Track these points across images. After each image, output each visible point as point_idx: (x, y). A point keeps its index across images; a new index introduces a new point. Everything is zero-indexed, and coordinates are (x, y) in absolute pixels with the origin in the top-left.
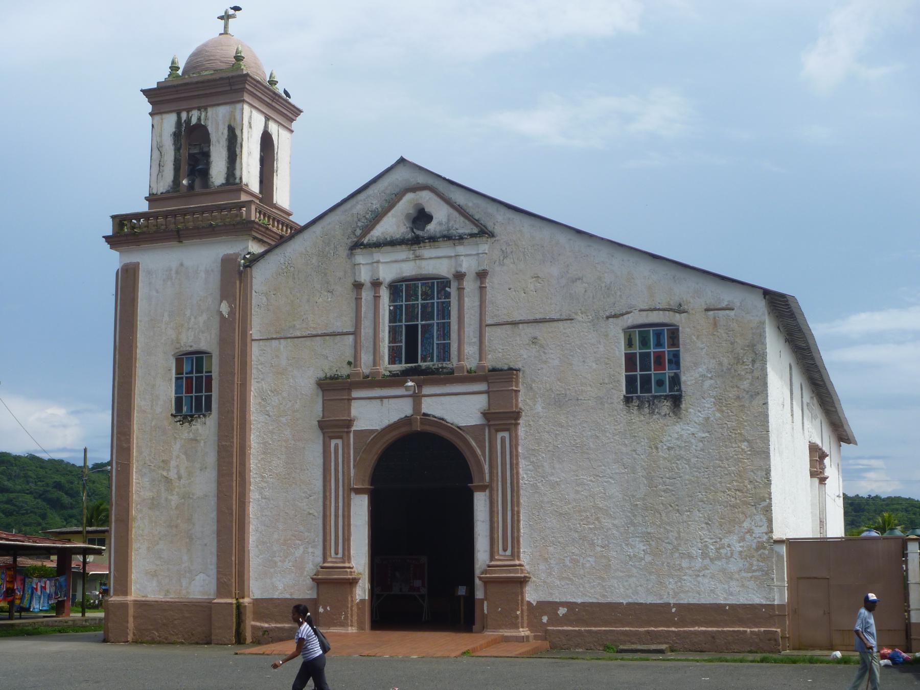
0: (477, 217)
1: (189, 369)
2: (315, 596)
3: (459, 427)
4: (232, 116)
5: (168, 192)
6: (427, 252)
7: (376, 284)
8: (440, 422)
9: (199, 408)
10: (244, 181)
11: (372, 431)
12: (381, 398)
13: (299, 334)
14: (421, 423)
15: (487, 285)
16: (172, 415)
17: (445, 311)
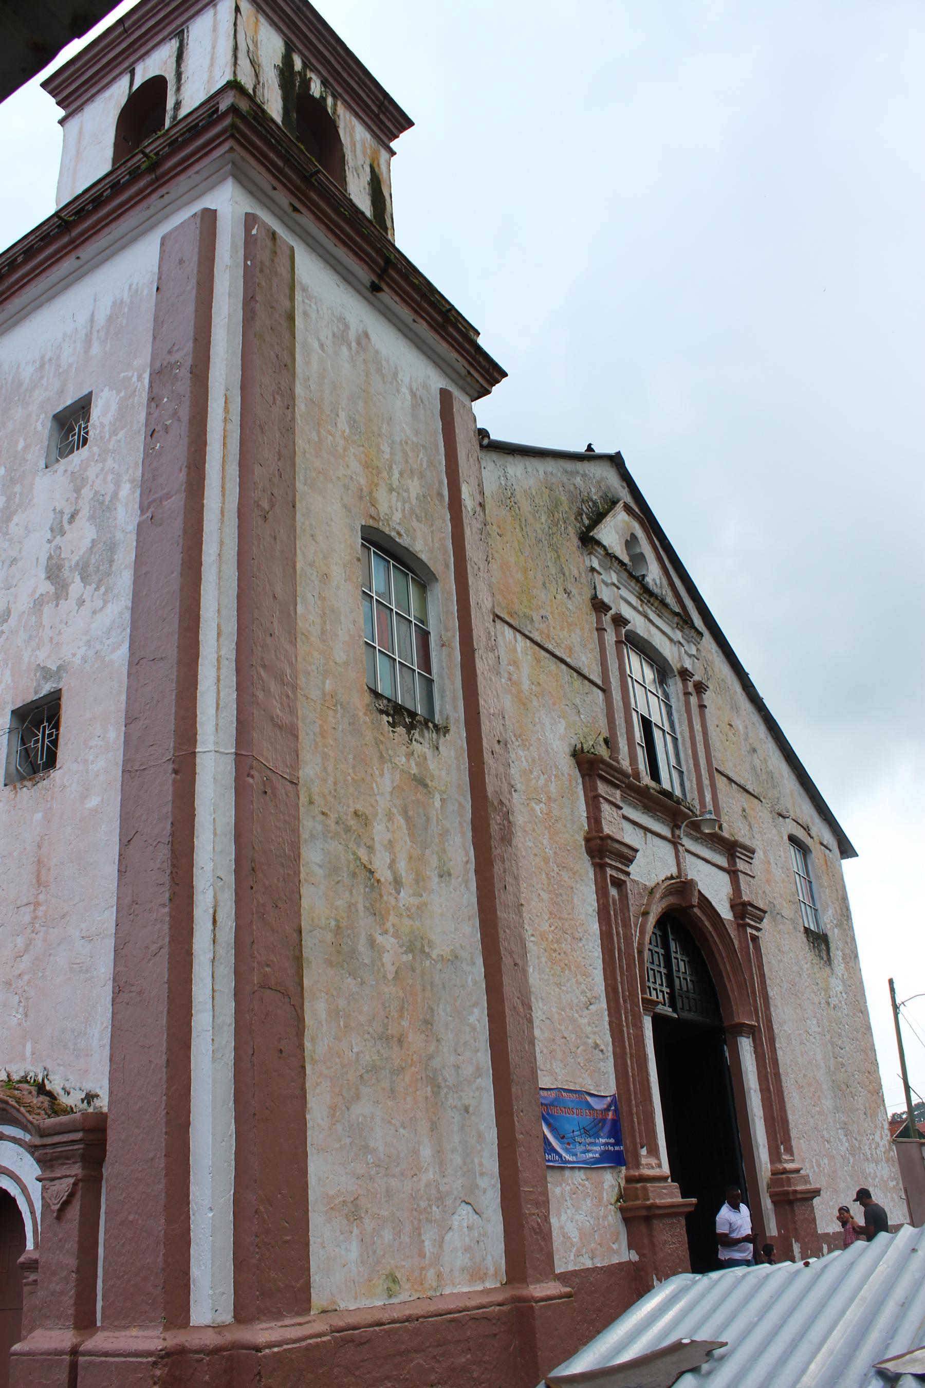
12: (647, 830)
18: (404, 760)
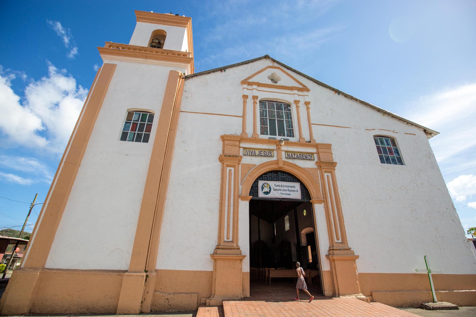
2: (210, 268)
7: (255, 97)
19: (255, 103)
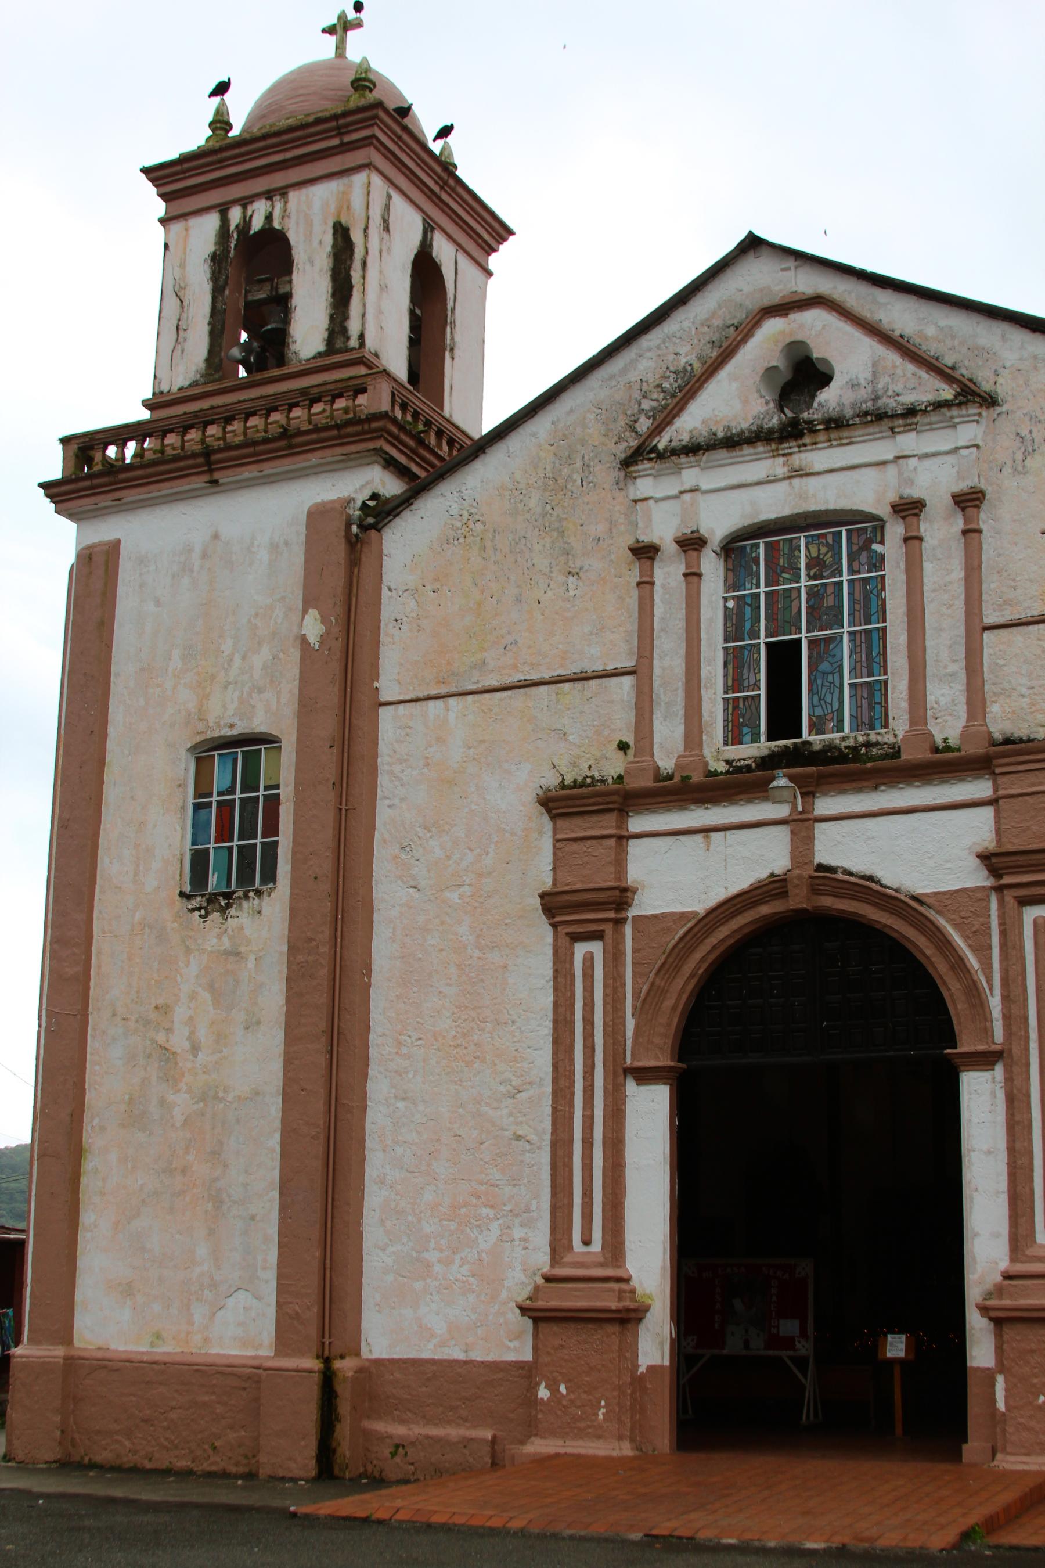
0: (948, 360)
1: (228, 783)
2: (527, 1356)
3: (914, 898)
4: (344, 202)
5: (194, 384)
6: (819, 458)
7: (692, 543)
8: (866, 888)
9: (246, 877)
10: (370, 343)
11: (683, 916)
13: (493, 682)
14: (815, 891)
15: (982, 526)
16: (182, 894)
17: (870, 601)
18: (215, 940)
19: (693, 576)
